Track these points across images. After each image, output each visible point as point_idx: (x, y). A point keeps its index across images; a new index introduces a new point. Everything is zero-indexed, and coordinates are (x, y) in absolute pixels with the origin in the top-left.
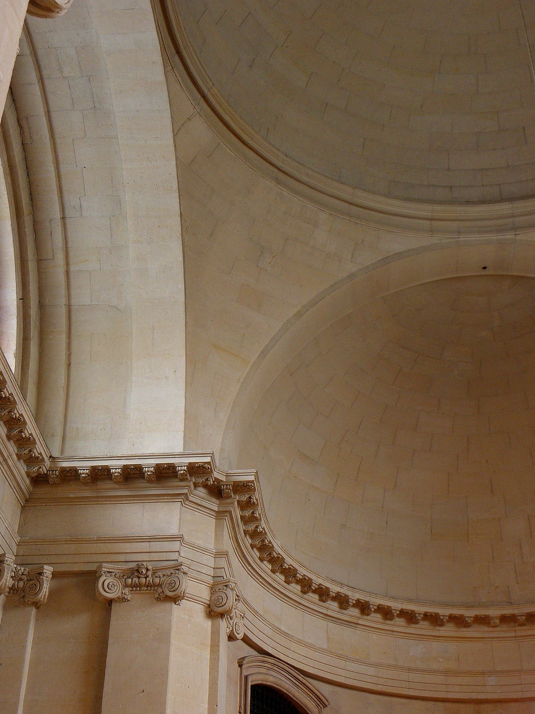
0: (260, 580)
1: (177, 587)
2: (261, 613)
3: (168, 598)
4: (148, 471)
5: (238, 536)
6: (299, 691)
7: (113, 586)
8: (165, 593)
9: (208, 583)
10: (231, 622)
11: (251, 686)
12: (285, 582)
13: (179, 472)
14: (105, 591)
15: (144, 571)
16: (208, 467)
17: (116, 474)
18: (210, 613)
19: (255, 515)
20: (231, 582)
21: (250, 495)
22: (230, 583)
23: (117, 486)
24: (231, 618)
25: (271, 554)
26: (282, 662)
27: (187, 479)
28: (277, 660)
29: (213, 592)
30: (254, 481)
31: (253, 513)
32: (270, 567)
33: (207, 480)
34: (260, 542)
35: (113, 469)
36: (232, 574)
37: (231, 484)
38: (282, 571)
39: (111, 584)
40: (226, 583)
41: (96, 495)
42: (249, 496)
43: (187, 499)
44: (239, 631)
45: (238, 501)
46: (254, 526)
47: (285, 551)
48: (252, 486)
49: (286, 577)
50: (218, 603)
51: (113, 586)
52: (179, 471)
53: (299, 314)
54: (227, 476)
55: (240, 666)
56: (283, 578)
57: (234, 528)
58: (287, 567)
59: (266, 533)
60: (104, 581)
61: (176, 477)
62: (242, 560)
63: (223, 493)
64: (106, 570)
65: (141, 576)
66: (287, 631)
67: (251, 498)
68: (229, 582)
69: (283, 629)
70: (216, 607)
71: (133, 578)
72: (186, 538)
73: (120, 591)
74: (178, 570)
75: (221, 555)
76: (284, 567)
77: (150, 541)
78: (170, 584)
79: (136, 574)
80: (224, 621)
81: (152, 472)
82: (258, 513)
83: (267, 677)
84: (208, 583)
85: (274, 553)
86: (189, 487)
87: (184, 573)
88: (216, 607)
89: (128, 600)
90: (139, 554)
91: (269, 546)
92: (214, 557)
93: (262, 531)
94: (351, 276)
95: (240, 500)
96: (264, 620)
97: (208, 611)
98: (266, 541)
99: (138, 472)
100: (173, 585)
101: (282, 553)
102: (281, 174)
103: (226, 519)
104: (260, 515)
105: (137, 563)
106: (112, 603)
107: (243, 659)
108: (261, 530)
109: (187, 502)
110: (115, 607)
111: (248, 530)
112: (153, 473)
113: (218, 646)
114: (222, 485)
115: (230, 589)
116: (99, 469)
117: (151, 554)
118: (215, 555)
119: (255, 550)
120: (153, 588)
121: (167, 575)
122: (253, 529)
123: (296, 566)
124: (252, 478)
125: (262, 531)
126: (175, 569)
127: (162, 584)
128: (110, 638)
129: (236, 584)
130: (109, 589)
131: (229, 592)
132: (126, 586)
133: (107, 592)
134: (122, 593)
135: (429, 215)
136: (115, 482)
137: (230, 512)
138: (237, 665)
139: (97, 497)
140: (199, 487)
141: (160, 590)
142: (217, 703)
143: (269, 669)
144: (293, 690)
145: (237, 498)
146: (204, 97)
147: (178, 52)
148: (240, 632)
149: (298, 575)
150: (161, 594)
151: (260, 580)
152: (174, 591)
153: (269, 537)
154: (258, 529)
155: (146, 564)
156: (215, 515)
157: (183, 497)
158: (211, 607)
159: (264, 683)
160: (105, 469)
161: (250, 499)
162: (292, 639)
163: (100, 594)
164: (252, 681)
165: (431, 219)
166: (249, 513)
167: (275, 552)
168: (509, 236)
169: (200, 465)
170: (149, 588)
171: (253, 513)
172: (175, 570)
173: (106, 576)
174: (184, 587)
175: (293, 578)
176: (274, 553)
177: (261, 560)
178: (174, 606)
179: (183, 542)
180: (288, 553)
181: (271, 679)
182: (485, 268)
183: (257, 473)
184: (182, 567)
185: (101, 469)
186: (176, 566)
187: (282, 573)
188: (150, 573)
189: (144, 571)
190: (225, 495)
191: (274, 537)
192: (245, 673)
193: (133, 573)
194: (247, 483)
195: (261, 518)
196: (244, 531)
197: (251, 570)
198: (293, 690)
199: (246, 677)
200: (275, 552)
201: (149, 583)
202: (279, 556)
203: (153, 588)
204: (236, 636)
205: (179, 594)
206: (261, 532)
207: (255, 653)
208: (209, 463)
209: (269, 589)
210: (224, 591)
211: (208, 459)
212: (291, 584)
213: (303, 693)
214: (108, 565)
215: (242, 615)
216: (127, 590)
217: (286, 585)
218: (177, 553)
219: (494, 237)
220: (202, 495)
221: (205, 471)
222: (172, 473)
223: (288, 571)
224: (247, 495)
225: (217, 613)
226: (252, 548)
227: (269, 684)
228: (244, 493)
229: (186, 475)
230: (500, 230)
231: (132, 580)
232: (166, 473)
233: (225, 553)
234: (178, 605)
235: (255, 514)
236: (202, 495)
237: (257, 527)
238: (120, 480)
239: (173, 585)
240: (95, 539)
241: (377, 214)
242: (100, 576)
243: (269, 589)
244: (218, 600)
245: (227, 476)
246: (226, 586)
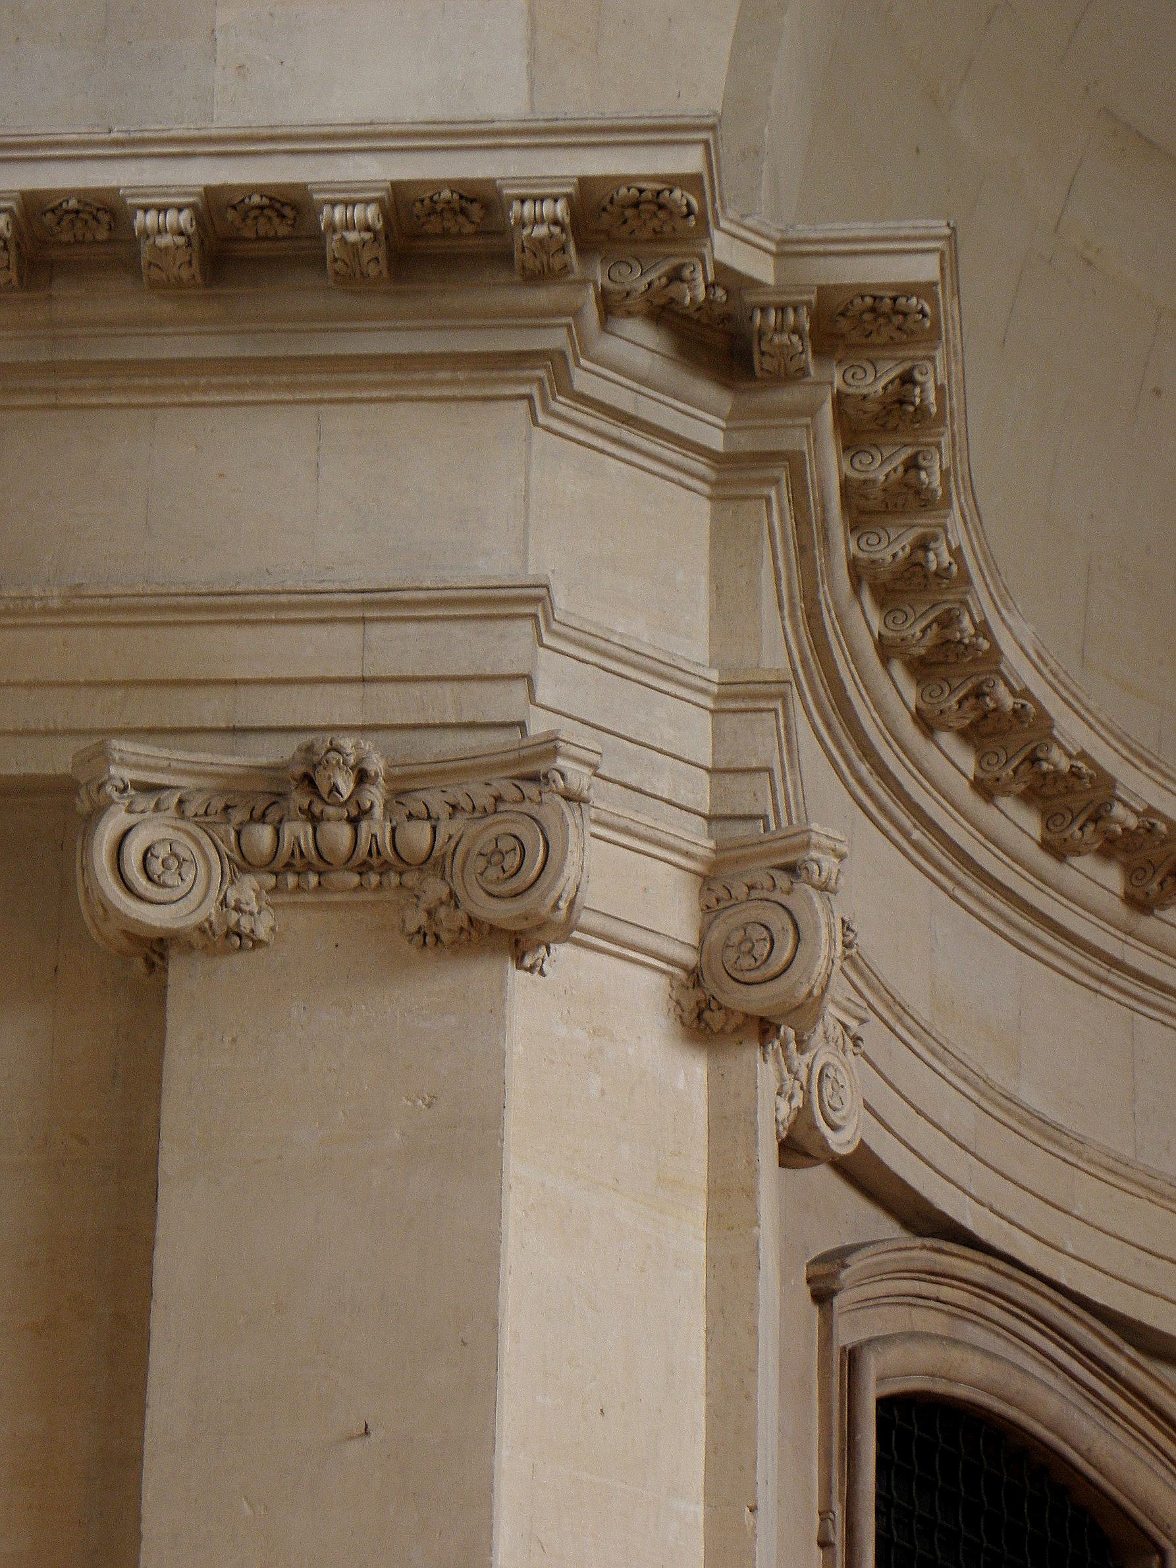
0: (916, 835)
1: (534, 873)
2: (923, 1011)
3: (480, 933)
4: (349, 226)
5: (821, 597)
6: (1113, 1429)
7: (173, 862)
8: (467, 905)
9: (687, 854)
10: (800, 1062)
11: (885, 1404)
12: (1045, 846)
13: (526, 232)
14: (128, 887)
15: (346, 785)
16: (688, 204)
17: (165, 241)
18: (699, 1017)
19: (923, 475)
20: (818, 847)
21: (907, 365)
22: (814, 854)
23: (167, 309)
24: (802, 1046)
25: (984, 694)
26: (1031, 1281)
27: (566, 268)
28: (1002, 1266)
29: (718, 900)
30: (935, 284)
31: (912, 465)
32: (968, 761)
33: (675, 276)
34: (929, 626)
35: (146, 209)
36: (797, 803)
37: (808, 304)
38: (1029, 788)
39: (162, 852)
40: (784, 851)
41: (44, 357)
42: (898, 371)
43: (562, 385)
44: (839, 1114)
45: (840, 400)
46: (910, 537)
47: (1055, 676)
48: (922, 312)
49: (1048, 819)
50: (747, 962)
51: (173, 862)
52: (524, 226)
54: (787, 251)
55: (822, 1296)
56: (1032, 823)
57: (803, 550)
58: (1064, 764)
59: (968, 581)
60: (125, 834)
61: (505, 258)
62: (829, 726)
63: (756, 356)
64: (129, 775)
65: (331, 811)
66: (1052, 1114)
67: (914, 383)
68: (807, 846)
69: (1031, 1097)
70: (737, 981)
71: (280, 821)
72: (561, 601)
73: (214, 893)
74: (533, 778)
75: (754, 697)
76: (1045, 766)
77: (364, 620)
78: (496, 858)
79: (299, 799)
80: (770, 1058)
81: (368, 228)
82: (941, 466)
83: (956, 1354)
84: (687, 854)
85: (1002, 689)
86: (577, 313)
87: (567, 799)
88: (737, 981)
89: (258, 943)
90: (305, 689)
91: (977, 648)
92: (711, 711)
93: (948, 569)
95: (851, 391)
96: (943, 1051)
97: (689, 1004)
98: (966, 622)
99: (283, 230)
100: (512, 861)
101: (1040, 691)
103: (768, 500)
104: (945, 474)
105: (306, 739)
106: (162, 957)
107: (839, 1257)
108: (946, 558)
109: (561, 405)
110: (177, 970)
111: (873, 562)
112: (376, 233)
113: (751, 1193)
114: (753, 308)
115: (814, 886)
116: (67, 212)
117: (373, 690)
118: (718, 697)
119: (898, 669)
120: (394, 879)
121: (474, 808)
122: (901, 554)
123: (1108, 759)
124: (925, 269)
125: (948, 569)
126: (515, 772)
127: (443, 856)
128: (165, 1144)
129: (841, 857)
130: (150, 879)
131: (805, 899)
132: (243, 864)
133: (140, 898)
134: (224, 903)
136: (154, 285)
137: (795, 463)
138: (806, 1291)
139: (52, 368)
140: (629, 314)
141: (436, 889)
142: (754, 1496)
143: (960, 1312)
144: (1085, 1425)
145: (838, 381)
148: (844, 1118)
149: (1118, 811)
150: (442, 912)
151: (916, 835)
152: (517, 895)
153: (982, 601)
154: (931, 556)
155: (356, 746)
156: (712, 475)
157: (541, 373)
158: (708, 983)
159: (940, 1387)
160: (98, 210)
161: (908, 386)
162: (1079, 1155)
163: (107, 908)
164: (881, 1380)
166: (888, 468)
167: (1008, 684)
169: (641, 191)
170: (374, 879)
171: (912, 465)
172: (517, 778)
173: (130, 811)
174: (570, 871)
175: (1091, 827)
176: (1002, 689)
177: (927, 724)
178: (517, 978)
179: (547, 624)
180: (1067, 688)
181: (976, 1366)
183: (952, 239)
184: (561, 762)
185: (77, 212)
186: (523, 760)
187: (1028, 797)
188: (375, 796)
189: (346, 785)
190: (769, 364)
191: (1001, 597)
192: (846, 1335)
193: (279, 795)
194: (894, 299)
195: (947, 494)
196: (854, 565)
197: (873, 782)
198: (1085, 1425)
199: (852, 1358)
200: (1008, 684)
201: (375, 850)
202: (1023, 706)
203: (394, 879)
204: (824, 1139)
205: (545, 911)
206: (942, 573)
207: (888, 1228)
208: (692, 182)
209: (959, 884)
210: (776, 896)
211: (690, 161)
212: (1075, 861)
213: (1133, 1444)
214: (143, 749)
215: (853, 1024)
216: (248, 889)
217: (1046, 862)
218: (520, 688)
220: (643, 361)
221: (667, 229)
222: (478, 234)
223: (1061, 785)
224: (892, 364)
225: (739, 1019)
226: (885, 661)
227: (961, 1391)
228: (872, 354)
229: (563, 249)
231: (277, 832)
232: (445, 234)
233: (773, 688)
234: (531, 969)
235: (925, 469)
236: (643, 361)
237: (923, 545)
238: (185, 274)
239: (512, 861)
240: (55, 604)
242: (98, 812)
243: (959, 884)
244: (746, 947)
245: (787, 251)
246: (791, 869)
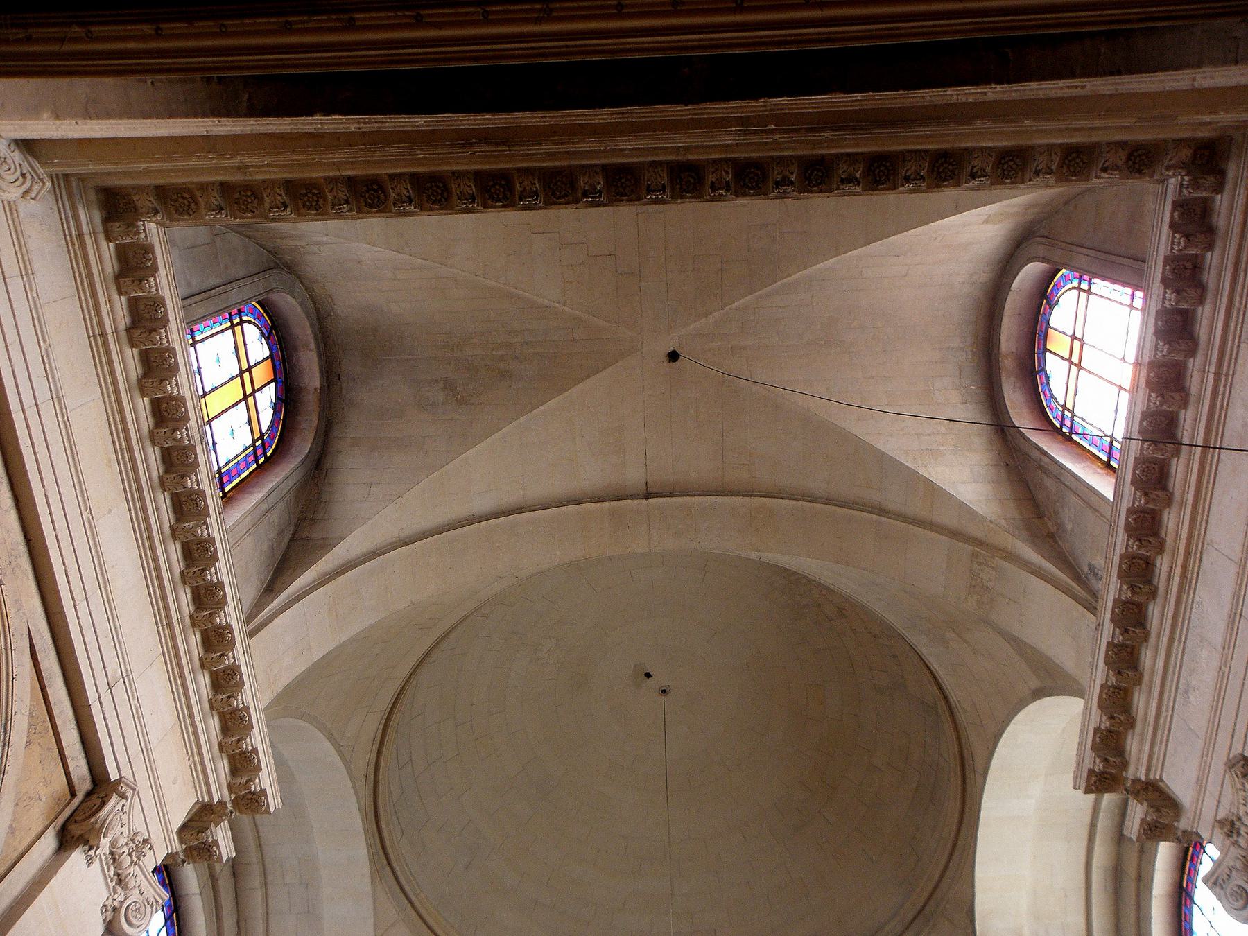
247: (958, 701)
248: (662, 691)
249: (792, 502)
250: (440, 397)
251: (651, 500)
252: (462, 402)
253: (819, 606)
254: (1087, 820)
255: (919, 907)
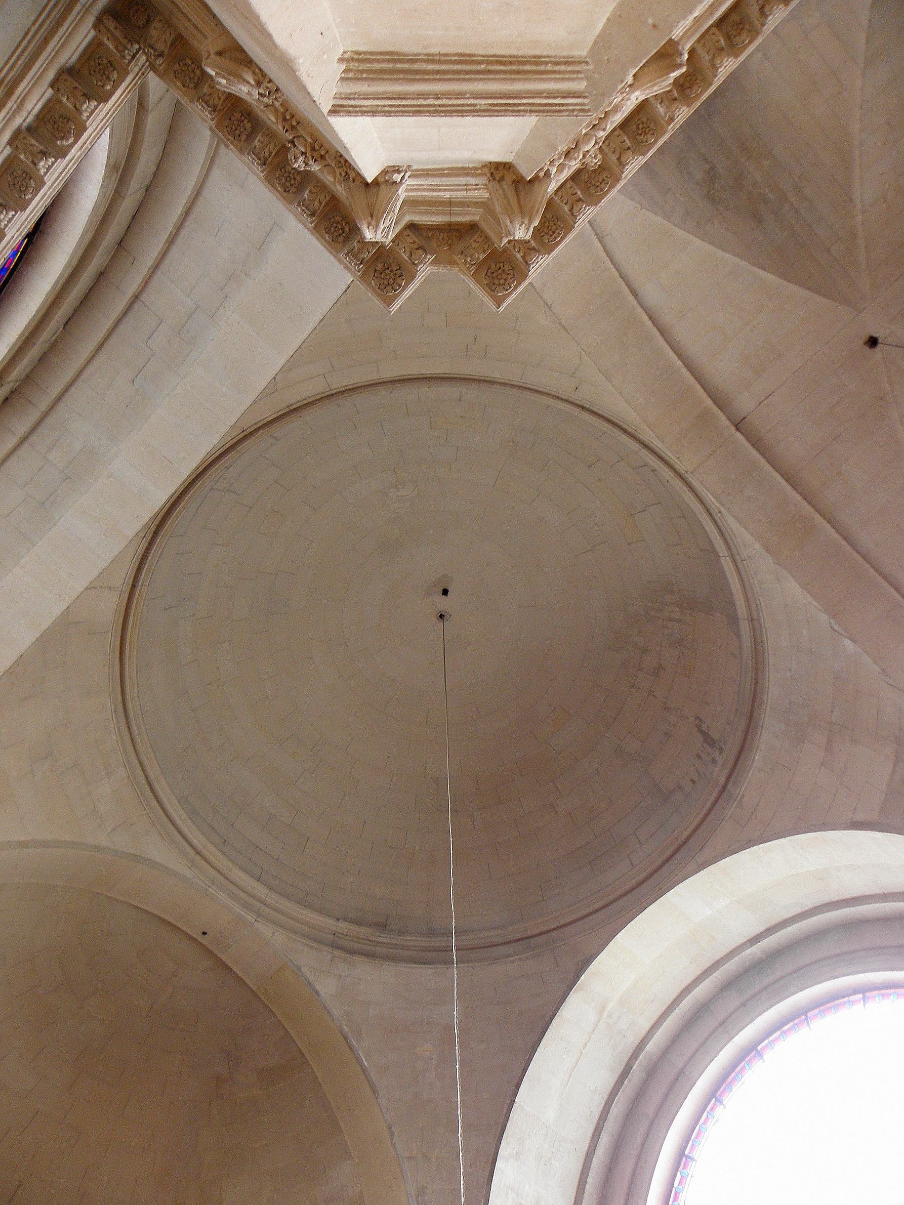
53: (24, 844)
94: (98, 848)
102: (120, 707)
135: (199, 847)
146: (134, 586)
147: (156, 533)
165: (199, 853)
168: (250, 918)
182: (204, 933)
219: (238, 909)
230: (246, 906)
241: (161, 811)
247: (743, 795)
248: (441, 618)
249: (837, 536)
250: (699, 175)
251: (738, 435)
252: (711, 197)
253: (645, 651)
254: (718, 956)
255: (529, 933)
